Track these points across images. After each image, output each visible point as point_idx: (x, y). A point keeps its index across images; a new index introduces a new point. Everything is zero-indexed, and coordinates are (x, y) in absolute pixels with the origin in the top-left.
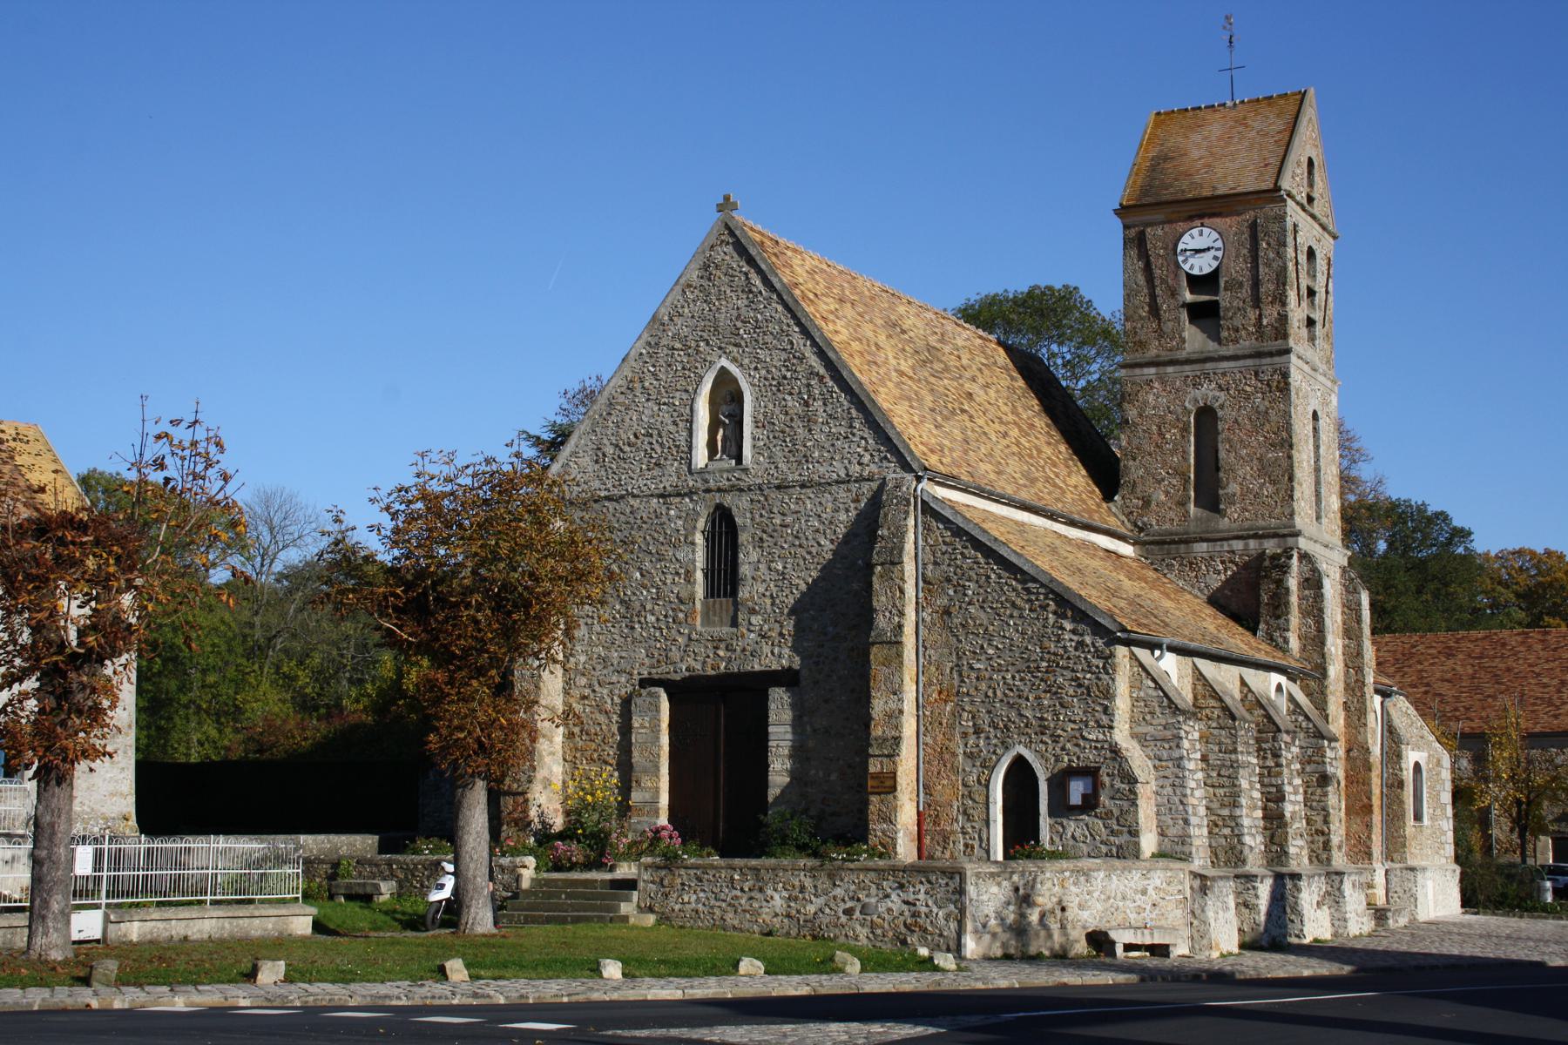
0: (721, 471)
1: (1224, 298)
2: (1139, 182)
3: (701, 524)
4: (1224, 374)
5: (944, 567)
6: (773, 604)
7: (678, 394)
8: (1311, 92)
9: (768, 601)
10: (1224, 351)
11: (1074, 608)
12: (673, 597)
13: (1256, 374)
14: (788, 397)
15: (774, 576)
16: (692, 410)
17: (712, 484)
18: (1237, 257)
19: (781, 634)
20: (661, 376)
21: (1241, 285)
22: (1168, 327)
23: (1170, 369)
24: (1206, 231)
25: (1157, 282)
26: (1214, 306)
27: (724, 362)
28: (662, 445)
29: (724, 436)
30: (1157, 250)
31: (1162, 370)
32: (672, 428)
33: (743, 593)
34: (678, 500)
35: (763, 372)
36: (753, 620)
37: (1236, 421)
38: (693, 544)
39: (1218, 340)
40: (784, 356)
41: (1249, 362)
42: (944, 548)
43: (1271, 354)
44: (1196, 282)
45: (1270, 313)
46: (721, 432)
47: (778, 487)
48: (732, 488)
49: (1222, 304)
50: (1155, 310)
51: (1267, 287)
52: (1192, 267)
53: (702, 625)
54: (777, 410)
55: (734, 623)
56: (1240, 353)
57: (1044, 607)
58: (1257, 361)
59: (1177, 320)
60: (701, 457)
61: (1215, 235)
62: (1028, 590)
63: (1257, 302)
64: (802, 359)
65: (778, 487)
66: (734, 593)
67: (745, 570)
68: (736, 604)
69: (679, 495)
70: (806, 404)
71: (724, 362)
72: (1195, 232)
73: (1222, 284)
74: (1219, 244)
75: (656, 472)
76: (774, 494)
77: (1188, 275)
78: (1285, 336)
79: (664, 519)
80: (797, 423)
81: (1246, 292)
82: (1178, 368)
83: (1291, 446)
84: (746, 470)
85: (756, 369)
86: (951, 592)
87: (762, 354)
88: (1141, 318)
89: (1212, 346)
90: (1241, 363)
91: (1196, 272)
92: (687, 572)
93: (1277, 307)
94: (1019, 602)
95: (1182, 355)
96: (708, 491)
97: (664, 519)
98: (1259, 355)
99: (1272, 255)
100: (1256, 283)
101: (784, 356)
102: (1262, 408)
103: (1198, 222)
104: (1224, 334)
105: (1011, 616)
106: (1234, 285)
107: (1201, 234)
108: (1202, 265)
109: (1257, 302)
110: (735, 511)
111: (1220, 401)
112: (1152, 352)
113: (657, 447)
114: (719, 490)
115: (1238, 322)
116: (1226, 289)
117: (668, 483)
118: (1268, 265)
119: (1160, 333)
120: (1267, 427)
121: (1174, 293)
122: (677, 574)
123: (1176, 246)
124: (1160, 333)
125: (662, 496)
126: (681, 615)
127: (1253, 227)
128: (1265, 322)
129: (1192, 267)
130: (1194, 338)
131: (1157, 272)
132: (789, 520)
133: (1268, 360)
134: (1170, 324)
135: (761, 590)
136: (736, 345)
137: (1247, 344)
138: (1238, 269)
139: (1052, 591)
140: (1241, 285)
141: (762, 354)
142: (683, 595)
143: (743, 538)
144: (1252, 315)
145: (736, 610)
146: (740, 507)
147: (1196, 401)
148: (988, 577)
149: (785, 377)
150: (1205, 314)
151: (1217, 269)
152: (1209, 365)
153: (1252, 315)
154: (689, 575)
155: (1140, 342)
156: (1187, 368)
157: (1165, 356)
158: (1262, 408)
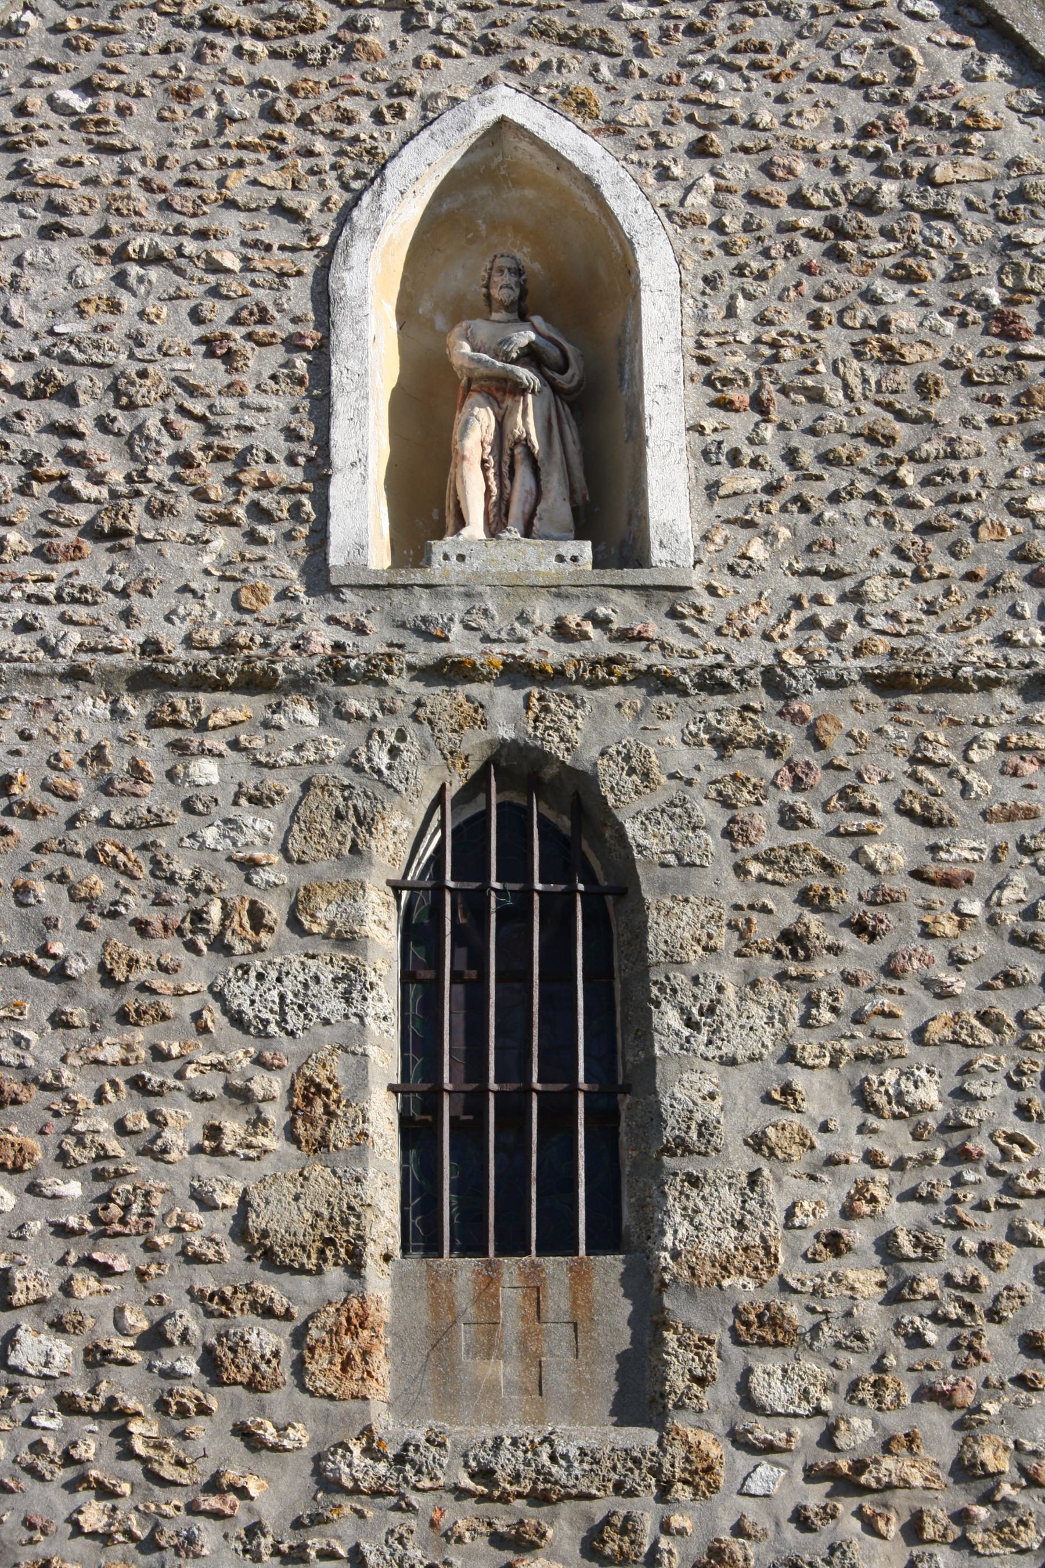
0: (515, 587)
3: (399, 839)
6: (895, 1296)
7: (231, 222)
9: (865, 1278)
12: (209, 1228)
14: (895, 293)
15: (894, 1139)
16: (323, 298)
17: (460, 645)
19: (966, 1470)
20: (128, 133)
27: (510, 103)
28: (134, 444)
29: (506, 453)
32: (206, 372)
33: (694, 1226)
34: (241, 707)
35: (740, 172)
36: (773, 1390)
38: (346, 939)
40: (856, 110)
46: (478, 429)
47: (889, 684)
48: (600, 673)
53: (404, 1405)
54: (834, 342)
55: (640, 1394)
60: (362, 520)
64: (964, 129)
65: (889, 684)
66: (620, 1226)
67: (697, 1085)
68: (645, 1289)
69: (253, 683)
70: (1004, 325)
71: (510, 103)
75: (95, 565)
76: (854, 716)
79: (153, 797)
80: (953, 404)
84: (670, 597)
85: (700, 149)
87: (730, 94)
92: (308, 1093)
96: (450, 672)
97: (153, 797)
101: (856, 110)
110: (614, 782)
113: (95, 445)
114: (517, 673)
117: (183, 617)
122: (241, 1095)
125: (146, 680)
126: (266, 1338)
132: (964, 849)
135: (821, 1205)
136: (576, 42)
141: (730, 94)
142: (280, 1217)
143: (671, 927)
145: (650, 1322)
146: (651, 769)
149: (869, 204)
154: (315, 1110)
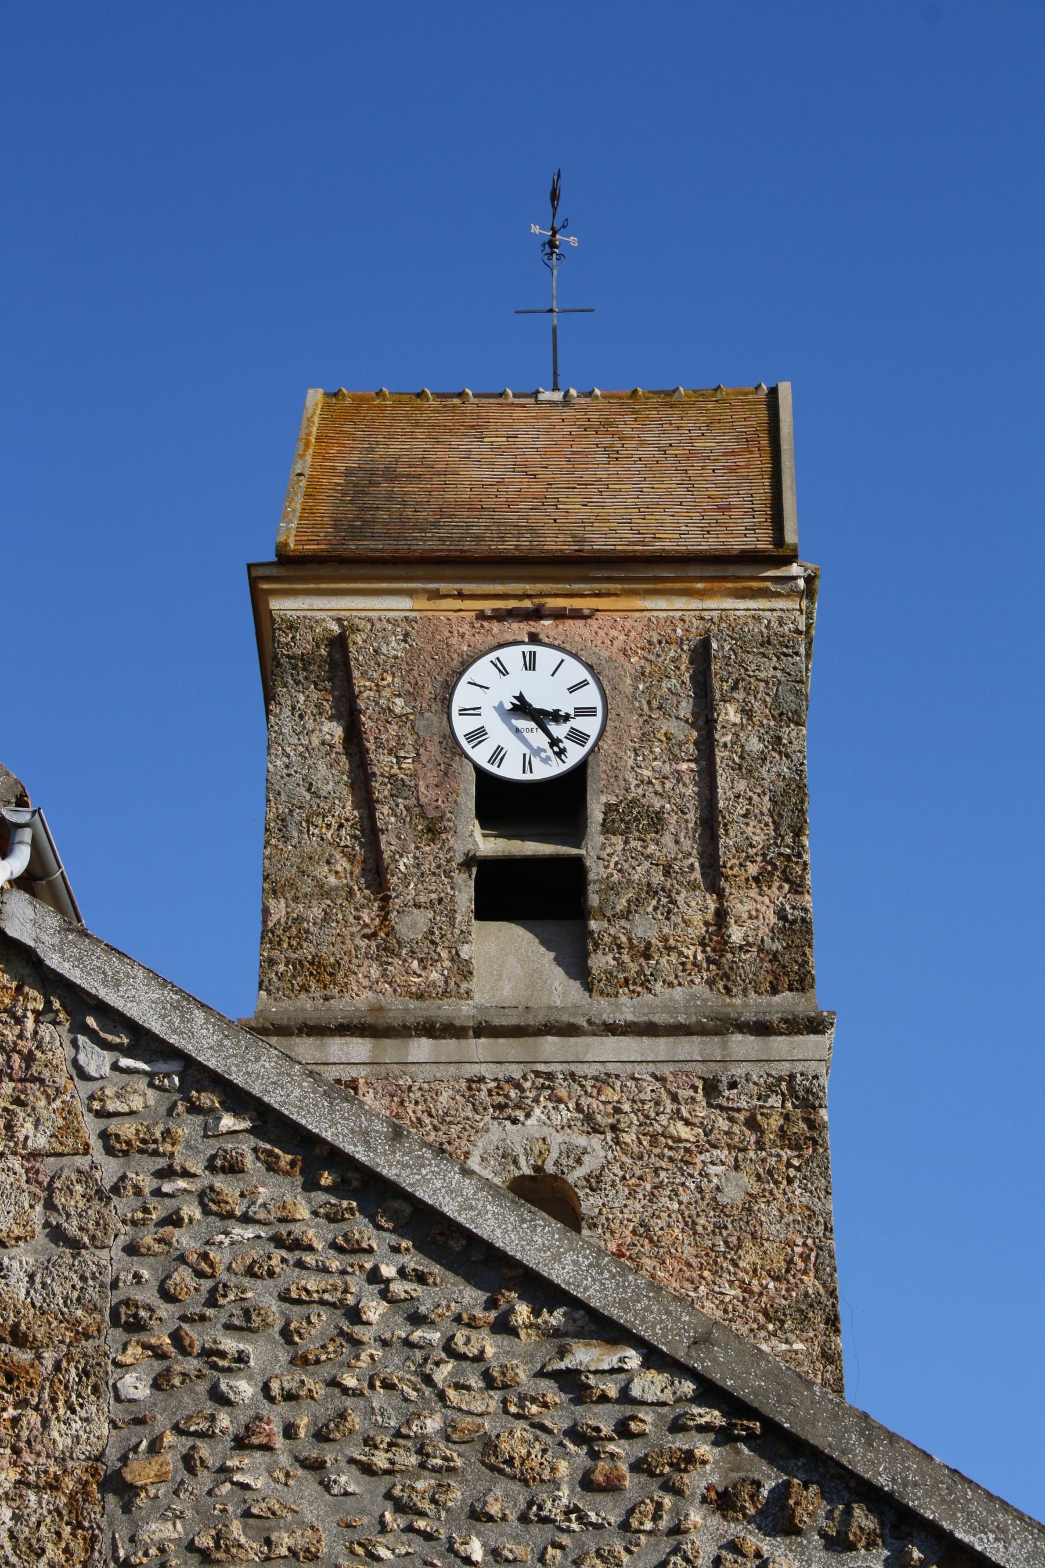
1: (600, 854)
2: (325, 509)
4: (603, 1081)
5: (110, 1258)
8: (785, 390)
10: (604, 1009)
11: (846, 1486)
13: (711, 1088)
18: (646, 738)
21: (657, 822)
22: (412, 925)
23: (421, 1049)
24: (547, 657)
25: (381, 790)
26: (576, 868)
30: (378, 692)
31: (390, 1049)
37: (643, 1230)
39: (578, 969)
41: (689, 1048)
42: (109, 1170)
43: (762, 1029)
44: (502, 802)
45: (754, 914)
49: (596, 871)
50: (376, 874)
51: (746, 832)
52: (498, 756)
56: (660, 1018)
57: (666, 1473)
58: (712, 1047)
59: (443, 905)
61: (574, 671)
62: (572, 1382)
63: (713, 876)
72: (512, 656)
73: (596, 813)
74: (590, 696)
77: (486, 781)
78: (802, 983)
81: (678, 841)
82: (449, 1046)
83: (833, 1322)
86: (135, 1385)
88: (324, 891)
89: (560, 991)
90: (660, 1047)
91: (511, 770)
93: (777, 892)
94: (516, 1441)
95: (464, 1011)
98: (723, 1026)
99: (754, 745)
100: (710, 823)
102: (733, 1195)
103: (520, 629)
104: (600, 962)
105: (478, 1516)
106: (635, 819)
107: (530, 663)
108: (521, 758)
109: (713, 876)
111: (590, 1164)
112: (357, 999)
115: (645, 927)
116: (607, 829)
118: (745, 767)
119: (386, 944)
120: (749, 1257)
121: (434, 830)
123: (450, 688)
124: (386, 944)
127: (702, 655)
128: (736, 935)
129: (498, 756)
130: (509, 963)
131: (382, 762)
133: (742, 1045)
134: (422, 919)
137: (679, 996)
138: (653, 772)
139: (709, 1392)
140: (657, 822)
144: (696, 908)
147: (508, 1157)
148: (355, 1315)
150: (538, 895)
151: (580, 770)
152: (550, 1046)
153: (696, 908)
155: (316, 962)
156: (479, 1047)
157: (400, 1007)
158: (733, 1195)
